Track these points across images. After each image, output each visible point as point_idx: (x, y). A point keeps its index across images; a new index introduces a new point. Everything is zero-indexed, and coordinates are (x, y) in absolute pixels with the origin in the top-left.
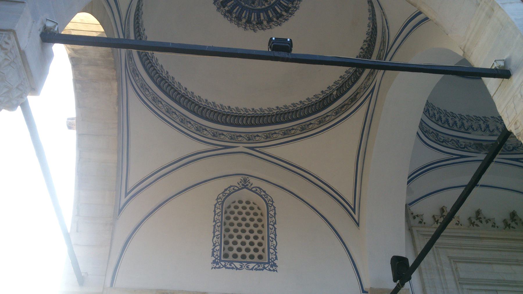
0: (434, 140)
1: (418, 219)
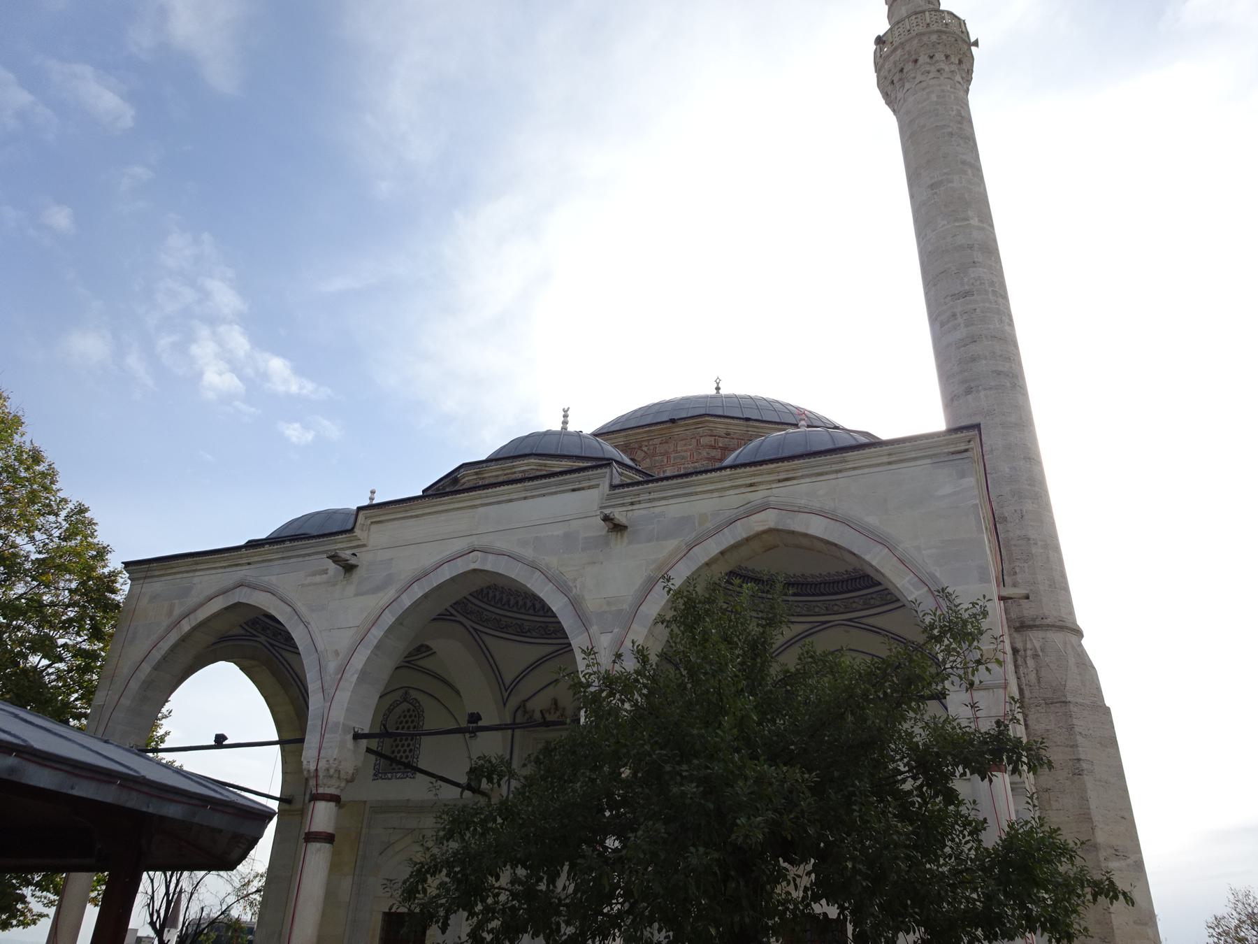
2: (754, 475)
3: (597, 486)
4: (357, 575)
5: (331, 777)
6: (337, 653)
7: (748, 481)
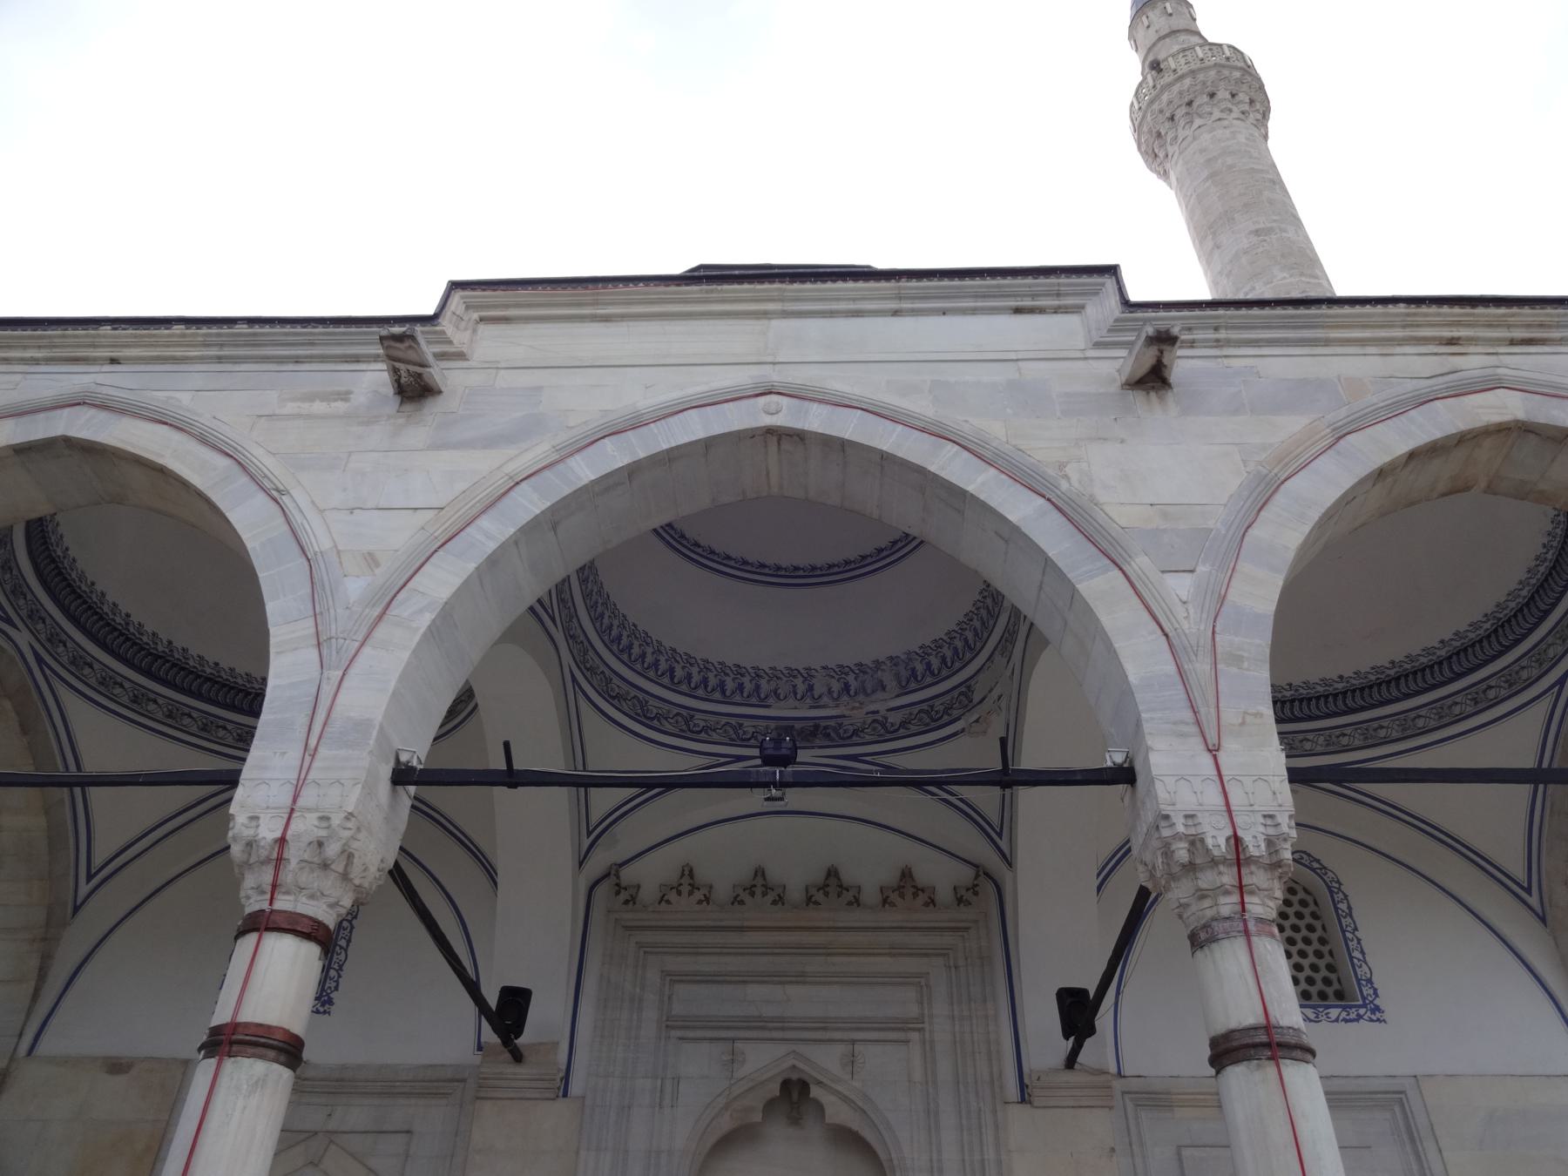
0: (676, 731)
1: (624, 896)
2: (1458, 324)
3: (1078, 309)
4: (433, 407)
5: (325, 866)
6: (371, 560)
7: (1447, 333)
